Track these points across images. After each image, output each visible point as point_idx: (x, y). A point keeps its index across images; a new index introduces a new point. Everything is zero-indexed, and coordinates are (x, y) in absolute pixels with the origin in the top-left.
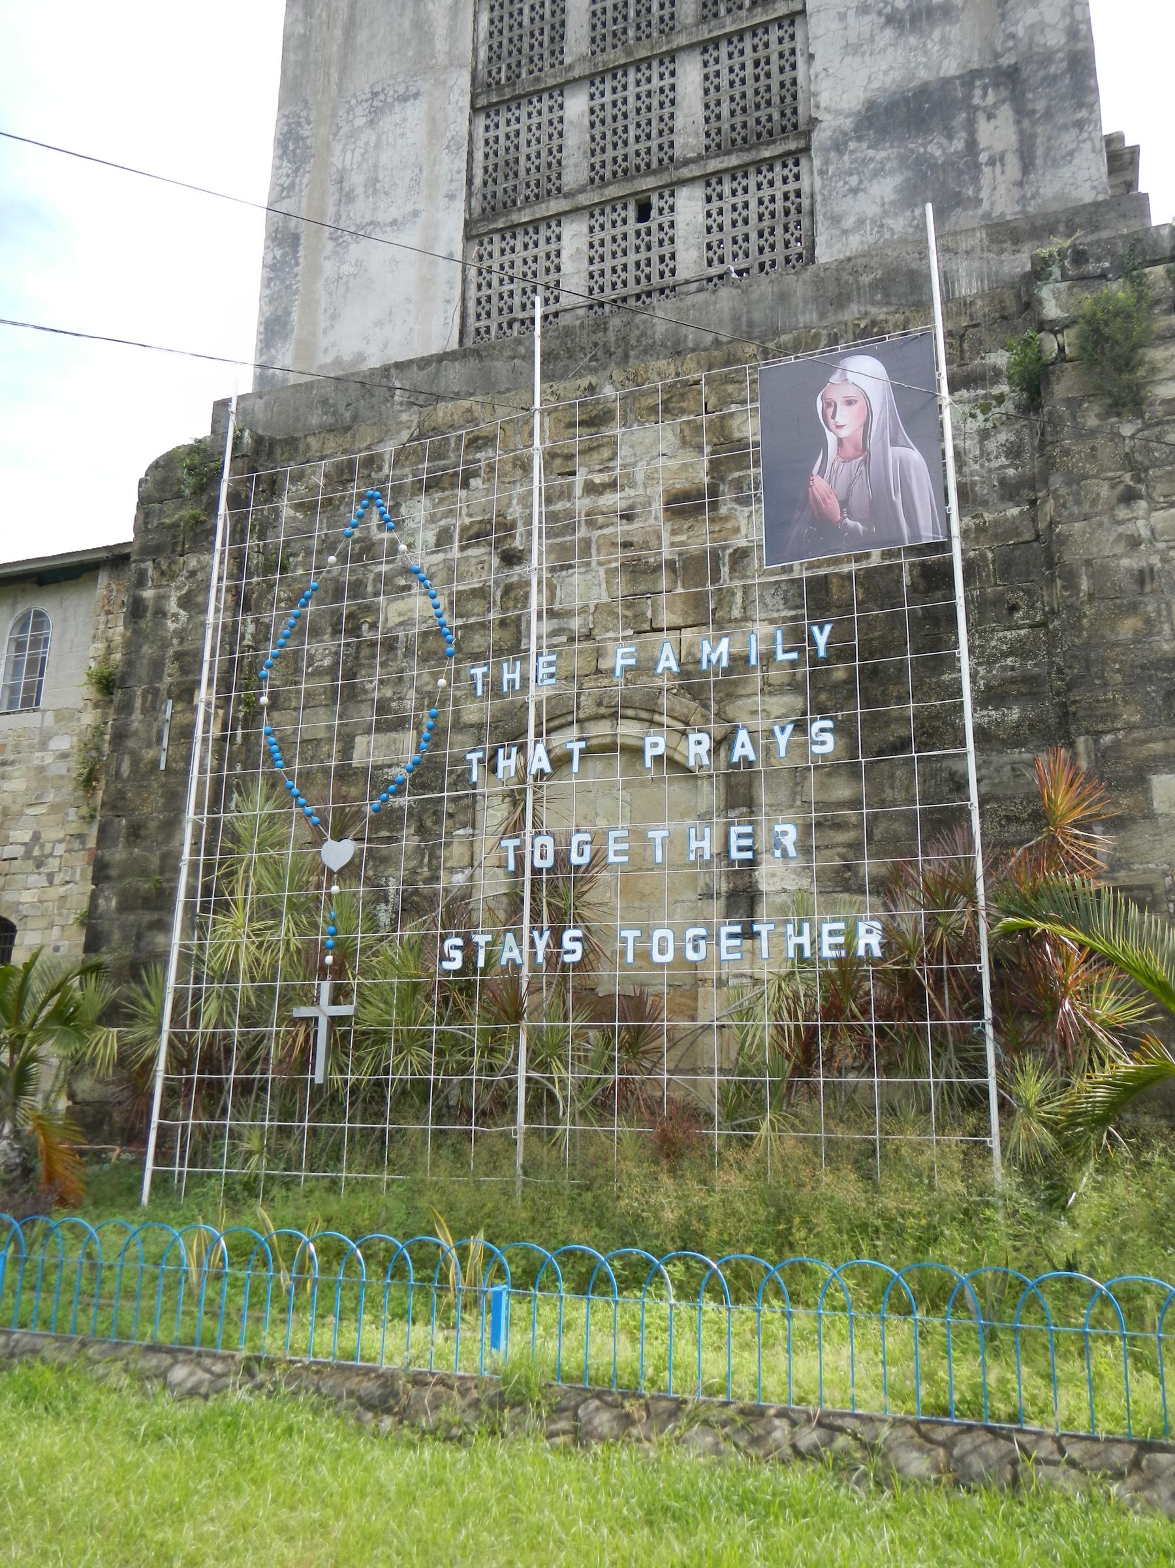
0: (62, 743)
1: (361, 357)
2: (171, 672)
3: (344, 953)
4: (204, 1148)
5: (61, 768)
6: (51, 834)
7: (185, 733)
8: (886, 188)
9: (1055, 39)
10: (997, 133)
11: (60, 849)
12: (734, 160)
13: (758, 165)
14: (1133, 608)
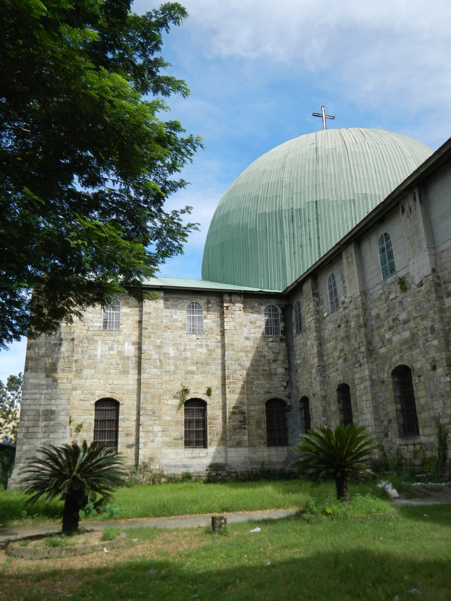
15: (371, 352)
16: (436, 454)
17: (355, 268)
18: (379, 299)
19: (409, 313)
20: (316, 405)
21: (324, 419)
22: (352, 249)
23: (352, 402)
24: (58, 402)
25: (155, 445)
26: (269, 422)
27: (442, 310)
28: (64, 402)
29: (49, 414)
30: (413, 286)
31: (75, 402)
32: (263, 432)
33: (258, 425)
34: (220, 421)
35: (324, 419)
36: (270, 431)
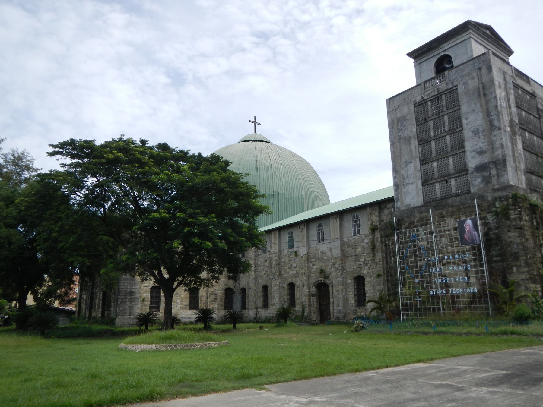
0: (366, 241)
1: (410, 204)
2: (392, 253)
3: (419, 292)
4: (407, 315)
5: (367, 246)
6: (368, 259)
7: (396, 262)
8: (479, 180)
9: (500, 157)
10: (494, 172)
11: (370, 262)
12: (458, 175)
13: (462, 175)
14: (510, 246)
15: (280, 275)
16: (301, 314)
17: (277, 241)
18: (286, 255)
19: (297, 265)
20: (250, 294)
22: (277, 232)
23: (269, 293)
24: (135, 287)
25: (177, 308)
26: (226, 299)
27: (308, 267)
28: (138, 287)
29: (132, 293)
30: (300, 257)
31: (142, 287)
33: (221, 301)
34: (205, 298)
36: (226, 303)
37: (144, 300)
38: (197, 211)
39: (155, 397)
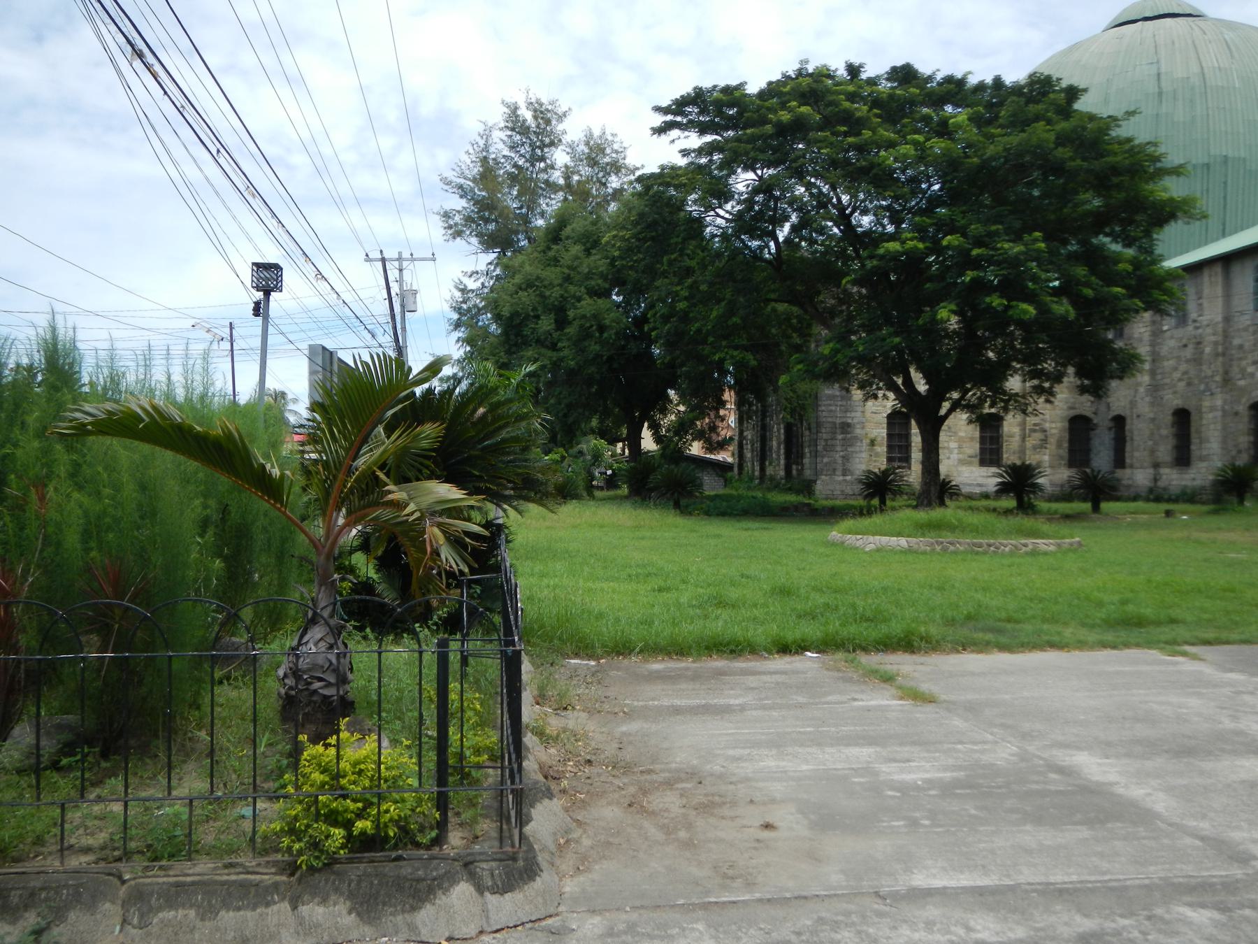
15: (1227, 381)
17: (1219, 290)
18: (1246, 329)
21: (1150, 443)
23: (1193, 429)
24: (853, 414)
25: (950, 462)
26: (1071, 441)
28: (858, 414)
29: (846, 427)
31: (868, 414)
32: (1064, 452)
33: (1059, 446)
34: (1017, 438)
35: (1150, 443)
36: (1071, 451)
37: (873, 443)
38: (994, 228)
39: (915, 644)
